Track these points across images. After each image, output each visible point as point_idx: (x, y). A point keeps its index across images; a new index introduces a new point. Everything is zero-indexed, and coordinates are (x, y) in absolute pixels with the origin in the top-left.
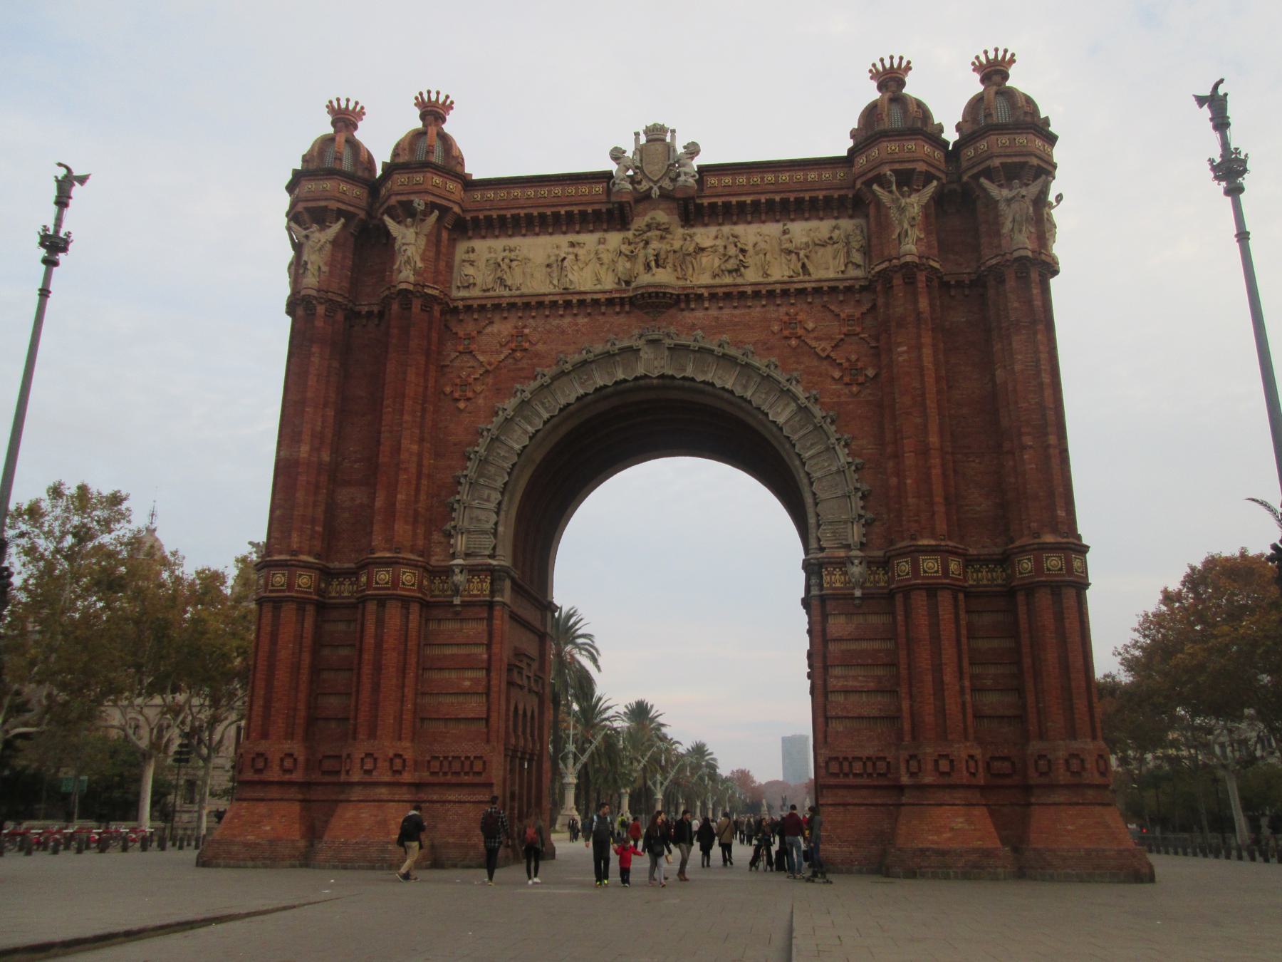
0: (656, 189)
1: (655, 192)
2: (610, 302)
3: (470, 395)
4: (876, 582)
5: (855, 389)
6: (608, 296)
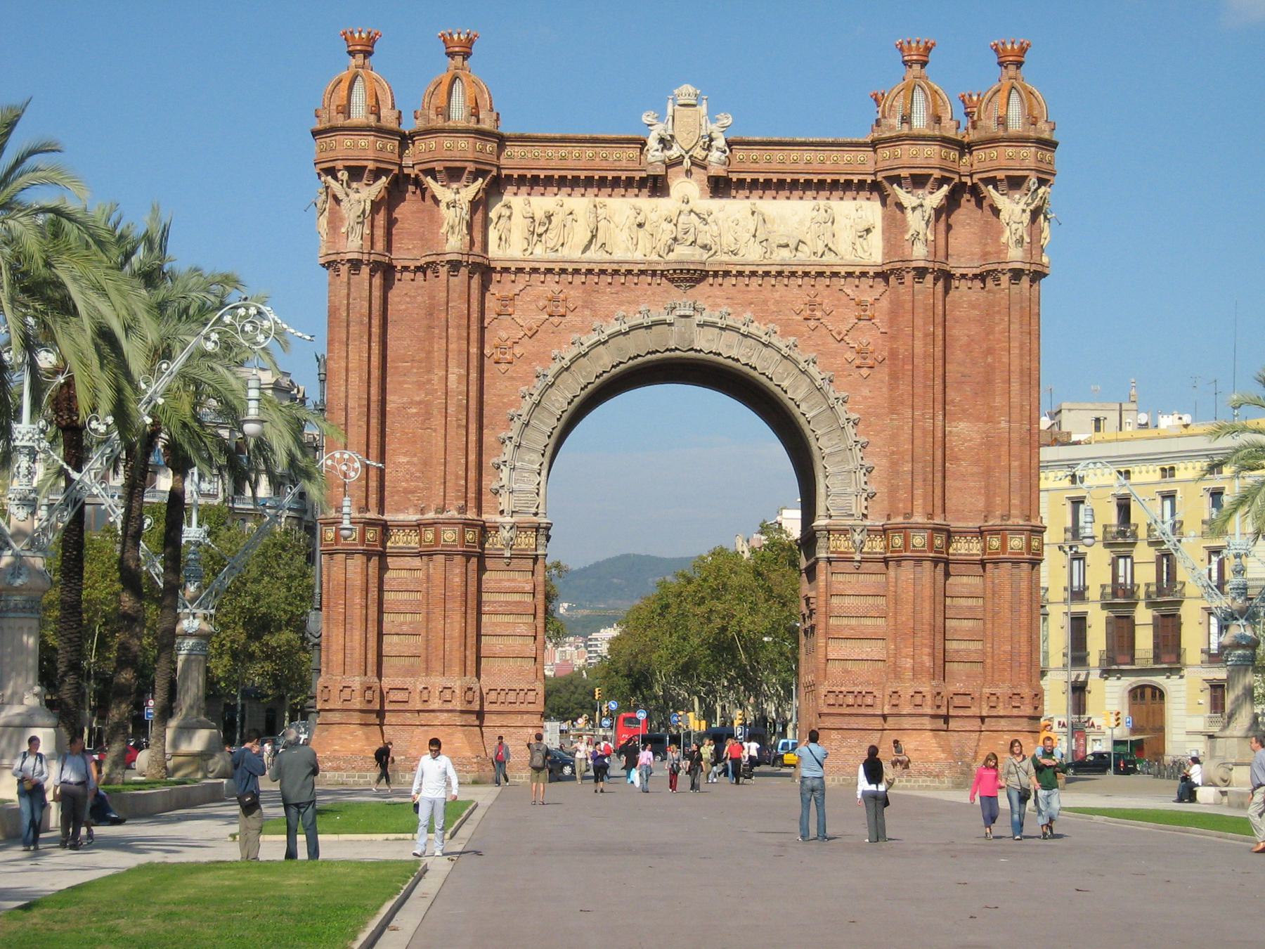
0: (687, 157)
1: (687, 163)
2: (642, 272)
3: (508, 357)
4: (872, 548)
5: (865, 372)
6: (643, 267)
